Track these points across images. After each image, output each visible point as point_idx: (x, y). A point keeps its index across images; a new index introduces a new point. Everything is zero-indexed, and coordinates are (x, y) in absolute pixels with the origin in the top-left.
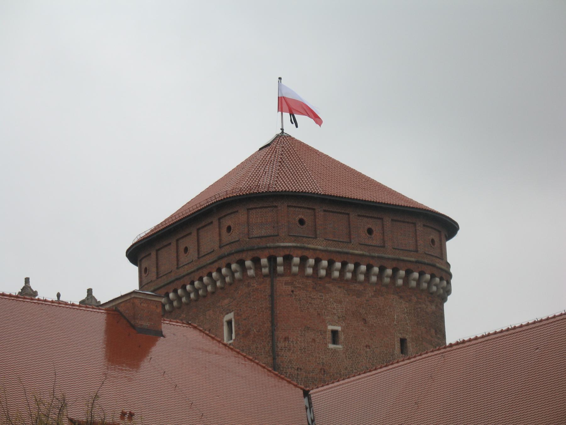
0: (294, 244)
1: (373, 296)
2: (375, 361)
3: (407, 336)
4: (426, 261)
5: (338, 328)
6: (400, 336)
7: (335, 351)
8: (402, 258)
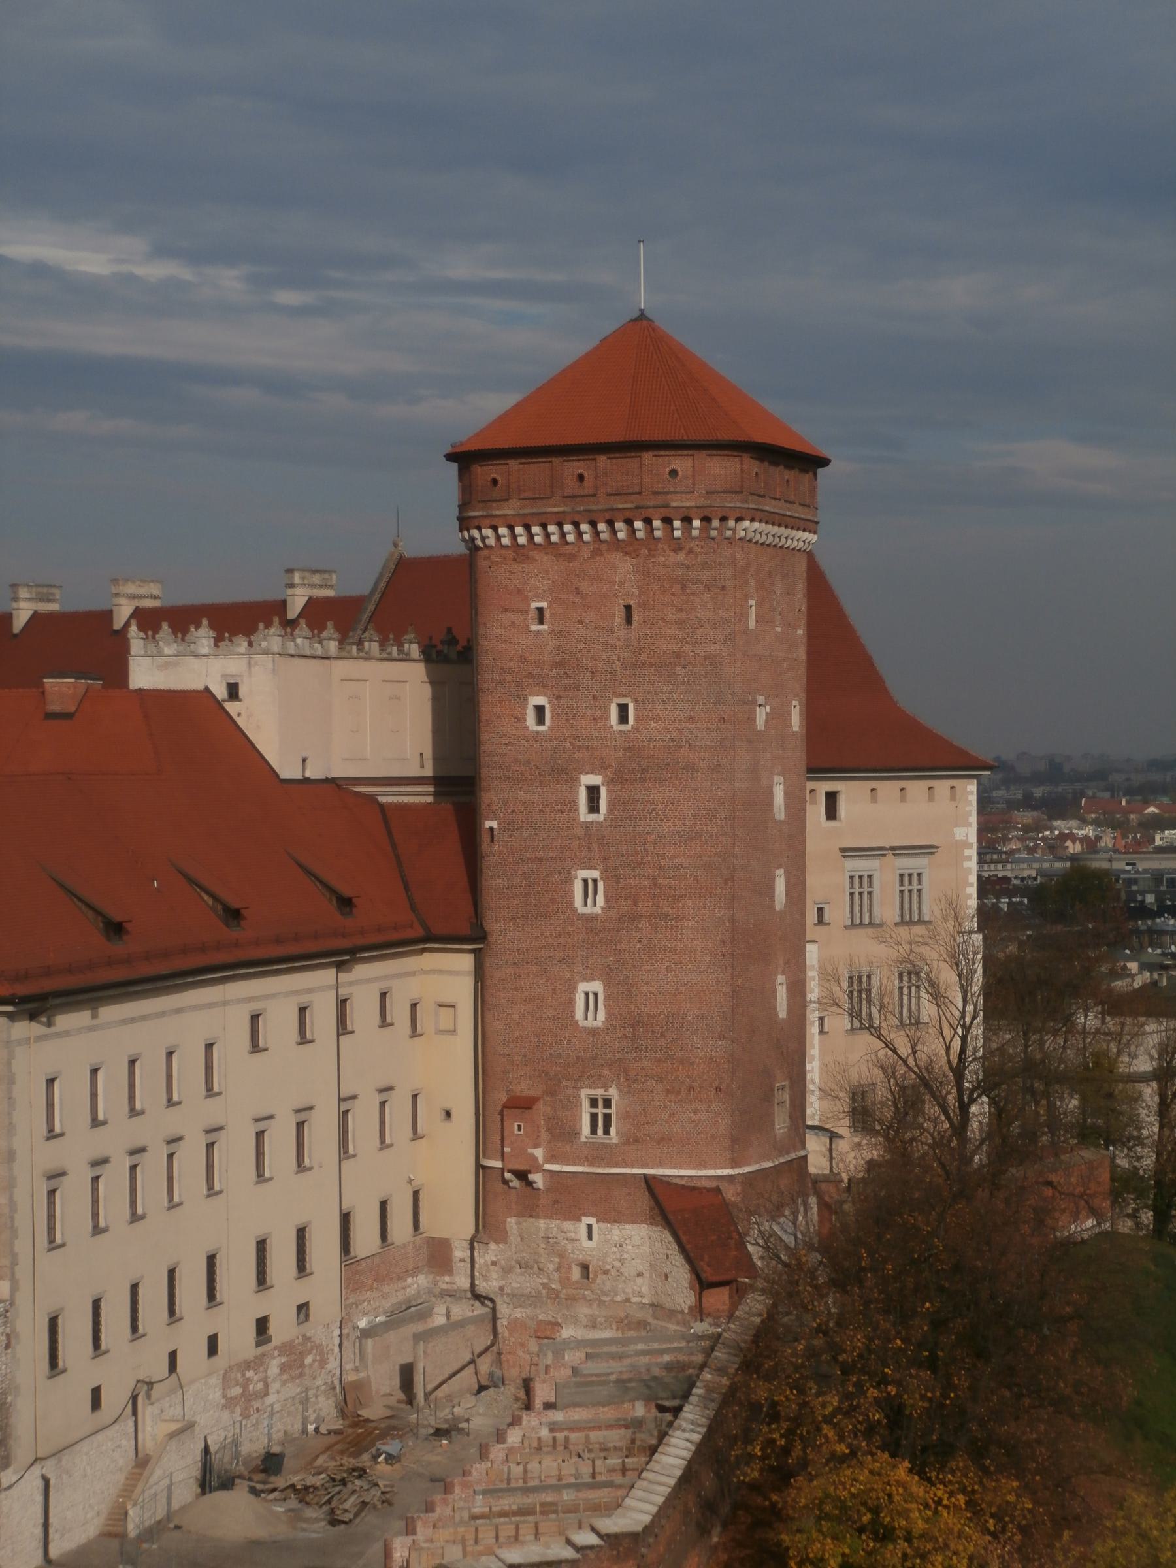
0: (480, 513)
1: (589, 558)
2: (589, 638)
3: (632, 602)
4: (651, 504)
5: (544, 605)
6: (623, 603)
7: (538, 633)
8: (615, 507)
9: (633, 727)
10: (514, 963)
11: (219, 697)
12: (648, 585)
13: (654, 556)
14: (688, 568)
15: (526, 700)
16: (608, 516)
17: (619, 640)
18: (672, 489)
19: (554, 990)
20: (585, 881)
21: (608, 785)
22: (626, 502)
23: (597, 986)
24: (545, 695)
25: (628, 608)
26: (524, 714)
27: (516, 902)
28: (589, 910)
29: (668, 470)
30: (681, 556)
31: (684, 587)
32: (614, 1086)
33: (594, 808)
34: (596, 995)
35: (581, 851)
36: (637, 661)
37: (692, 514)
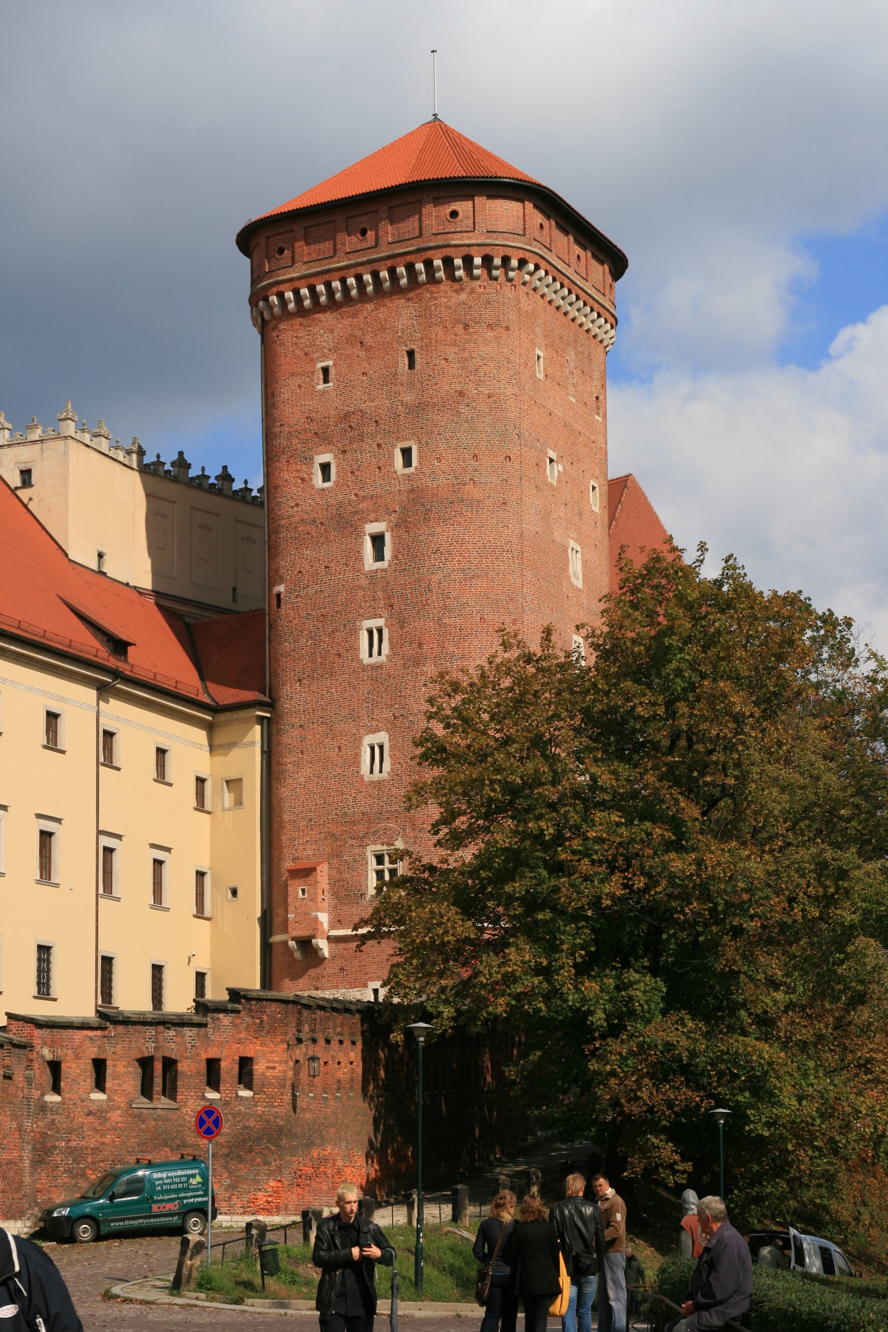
5: (330, 363)
7: (324, 392)
8: (396, 252)
9: (416, 469)
10: (301, 726)
11: (13, 487)
12: (430, 326)
13: (436, 298)
14: (470, 307)
15: (312, 459)
16: (389, 263)
17: (402, 385)
18: (453, 230)
19: (339, 748)
20: (370, 633)
21: (392, 531)
22: (407, 247)
23: (382, 737)
24: (331, 451)
25: (411, 354)
26: (310, 474)
27: (302, 663)
28: (375, 659)
29: (448, 211)
30: (463, 296)
31: (466, 327)
32: (400, 838)
33: (379, 556)
34: (381, 747)
35: (366, 601)
36: (420, 403)
37: (473, 251)
